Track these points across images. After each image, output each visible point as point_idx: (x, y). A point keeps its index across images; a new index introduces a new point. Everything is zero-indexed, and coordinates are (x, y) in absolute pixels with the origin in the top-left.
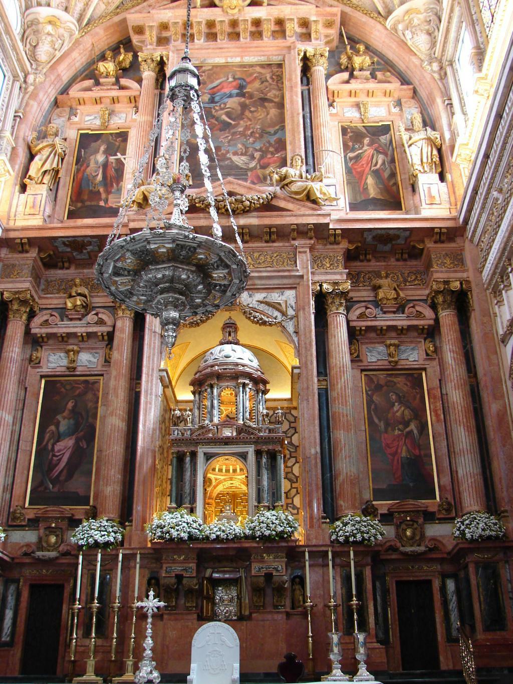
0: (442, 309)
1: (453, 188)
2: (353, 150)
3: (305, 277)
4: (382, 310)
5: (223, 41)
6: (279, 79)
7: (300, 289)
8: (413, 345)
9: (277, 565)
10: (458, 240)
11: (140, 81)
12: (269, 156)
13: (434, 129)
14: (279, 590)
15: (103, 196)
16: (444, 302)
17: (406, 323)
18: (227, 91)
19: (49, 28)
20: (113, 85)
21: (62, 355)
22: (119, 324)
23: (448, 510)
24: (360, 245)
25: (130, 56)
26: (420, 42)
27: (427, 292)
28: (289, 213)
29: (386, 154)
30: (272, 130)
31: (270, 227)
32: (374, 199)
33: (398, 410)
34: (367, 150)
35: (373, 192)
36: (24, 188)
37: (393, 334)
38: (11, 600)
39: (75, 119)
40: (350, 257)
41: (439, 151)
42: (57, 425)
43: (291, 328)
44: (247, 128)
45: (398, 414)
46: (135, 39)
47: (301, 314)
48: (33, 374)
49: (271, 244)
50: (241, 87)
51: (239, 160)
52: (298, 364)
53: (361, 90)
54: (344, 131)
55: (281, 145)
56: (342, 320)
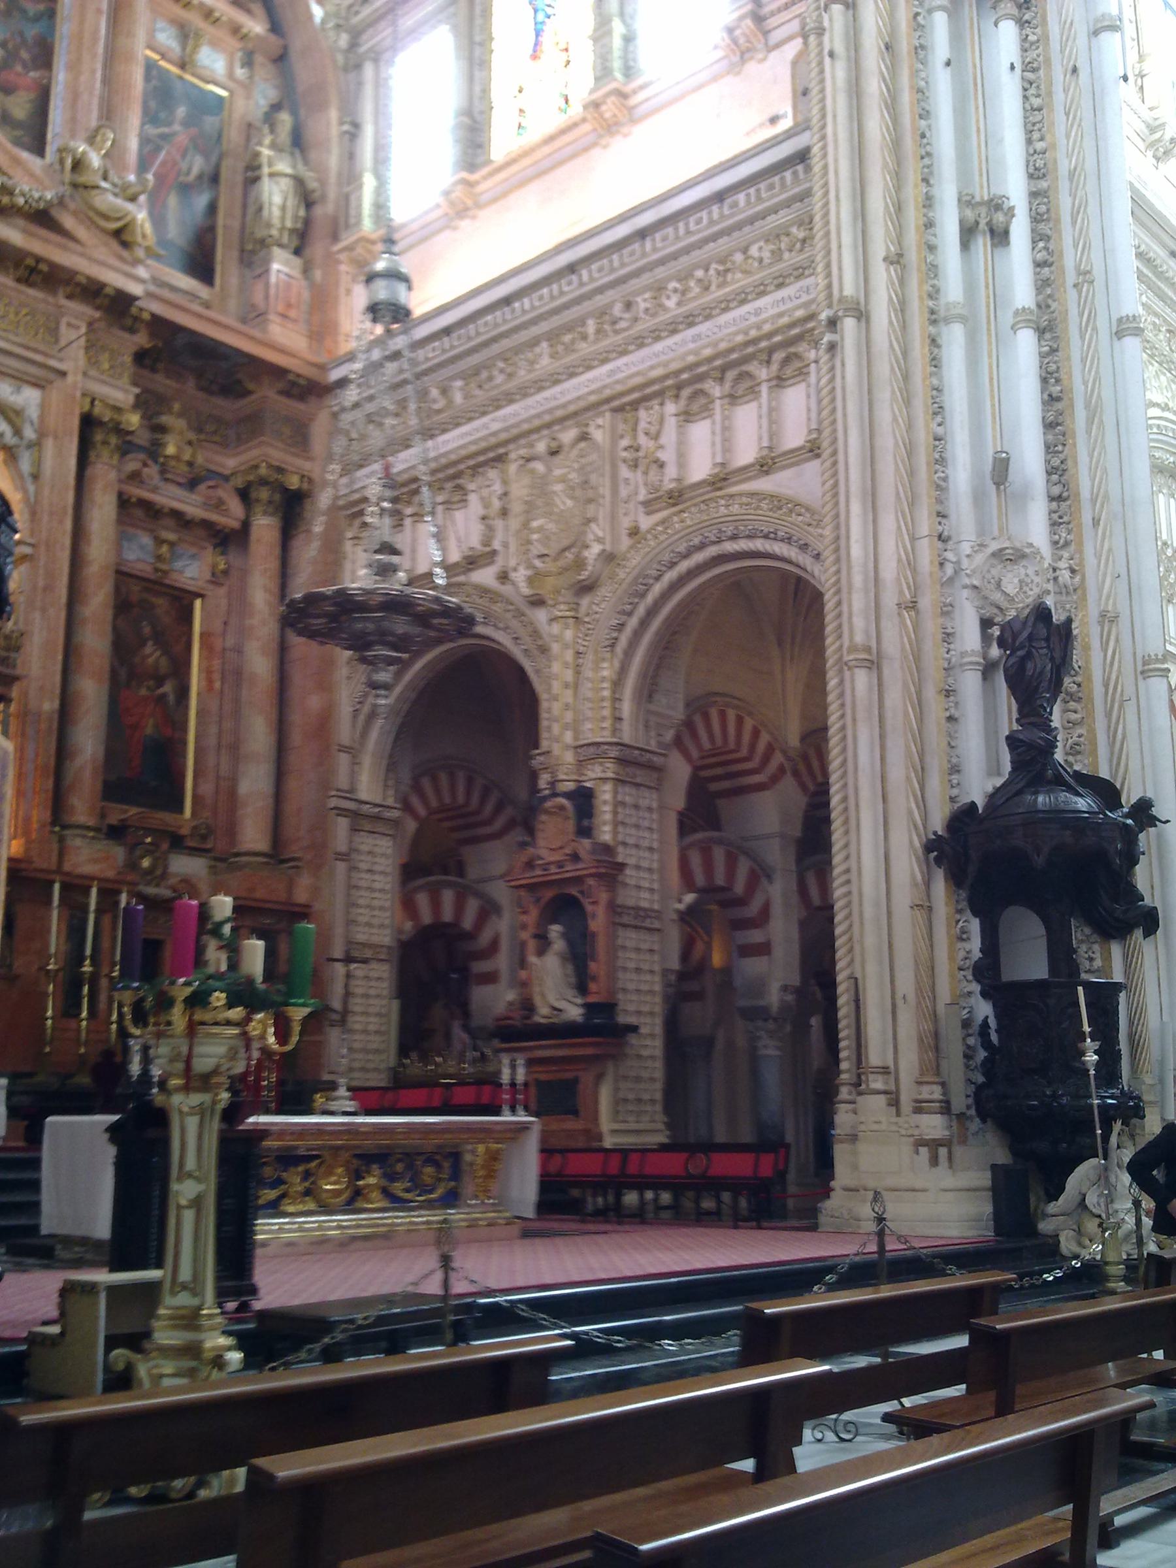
0: (265, 513)
3: (70, 379)
4: (163, 472)
7: (55, 395)
8: (193, 550)
12: (19, 68)
13: (306, 162)
16: (270, 502)
23: (204, 838)
24: (160, 345)
28: (78, 248)
31: (39, 260)
33: (151, 654)
43: (25, 465)
45: (151, 660)
47: (49, 445)
49: (23, 288)
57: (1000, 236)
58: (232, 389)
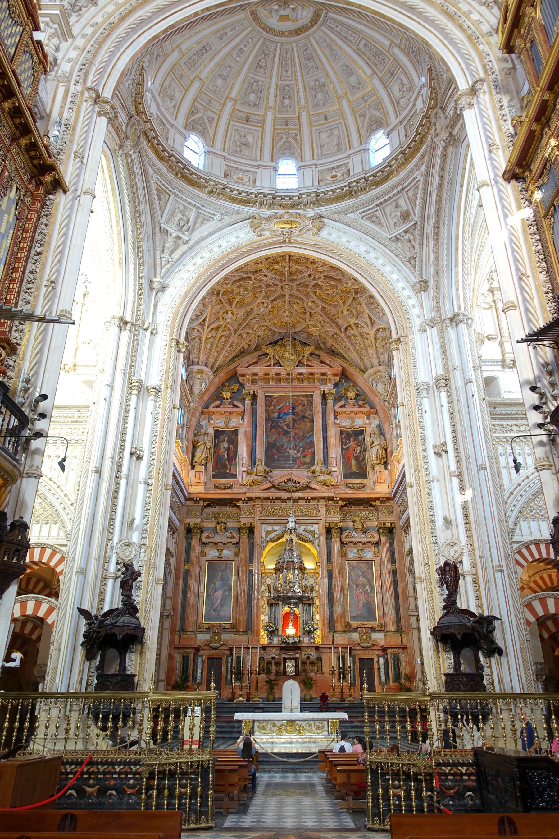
1: (391, 474)
2: (345, 445)
5: (284, 384)
6: (311, 404)
9: (311, 653)
10: (391, 502)
11: (242, 401)
14: (312, 663)
15: (228, 467)
17: (366, 541)
18: (286, 411)
19: (199, 376)
20: (230, 403)
21: (216, 551)
22: (242, 540)
25: (238, 385)
26: (380, 388)
27: (376, 523)
29: (361, 447)
30: (307, 435)
32: (355, 472)
33: (362, 580)
34: (352, 444)
35: (354, 469)
36: (193, 468)
37: (361, 544)
38: (200, 665)
39: (212, 422)
40: (342, 507)
41: (386, 450)
42: (215, 584)
43: (316, 542)
44: (296, 434)
46: (240, 379)
48: (203, 559)
50: (293, 409)
51: (292, 453)
52: (318, 560)
53: (351, 412)
54: (342, 432)
55: (312, 444)
56: (338, 539)
57: (446, 452)
58: (371, 505)
